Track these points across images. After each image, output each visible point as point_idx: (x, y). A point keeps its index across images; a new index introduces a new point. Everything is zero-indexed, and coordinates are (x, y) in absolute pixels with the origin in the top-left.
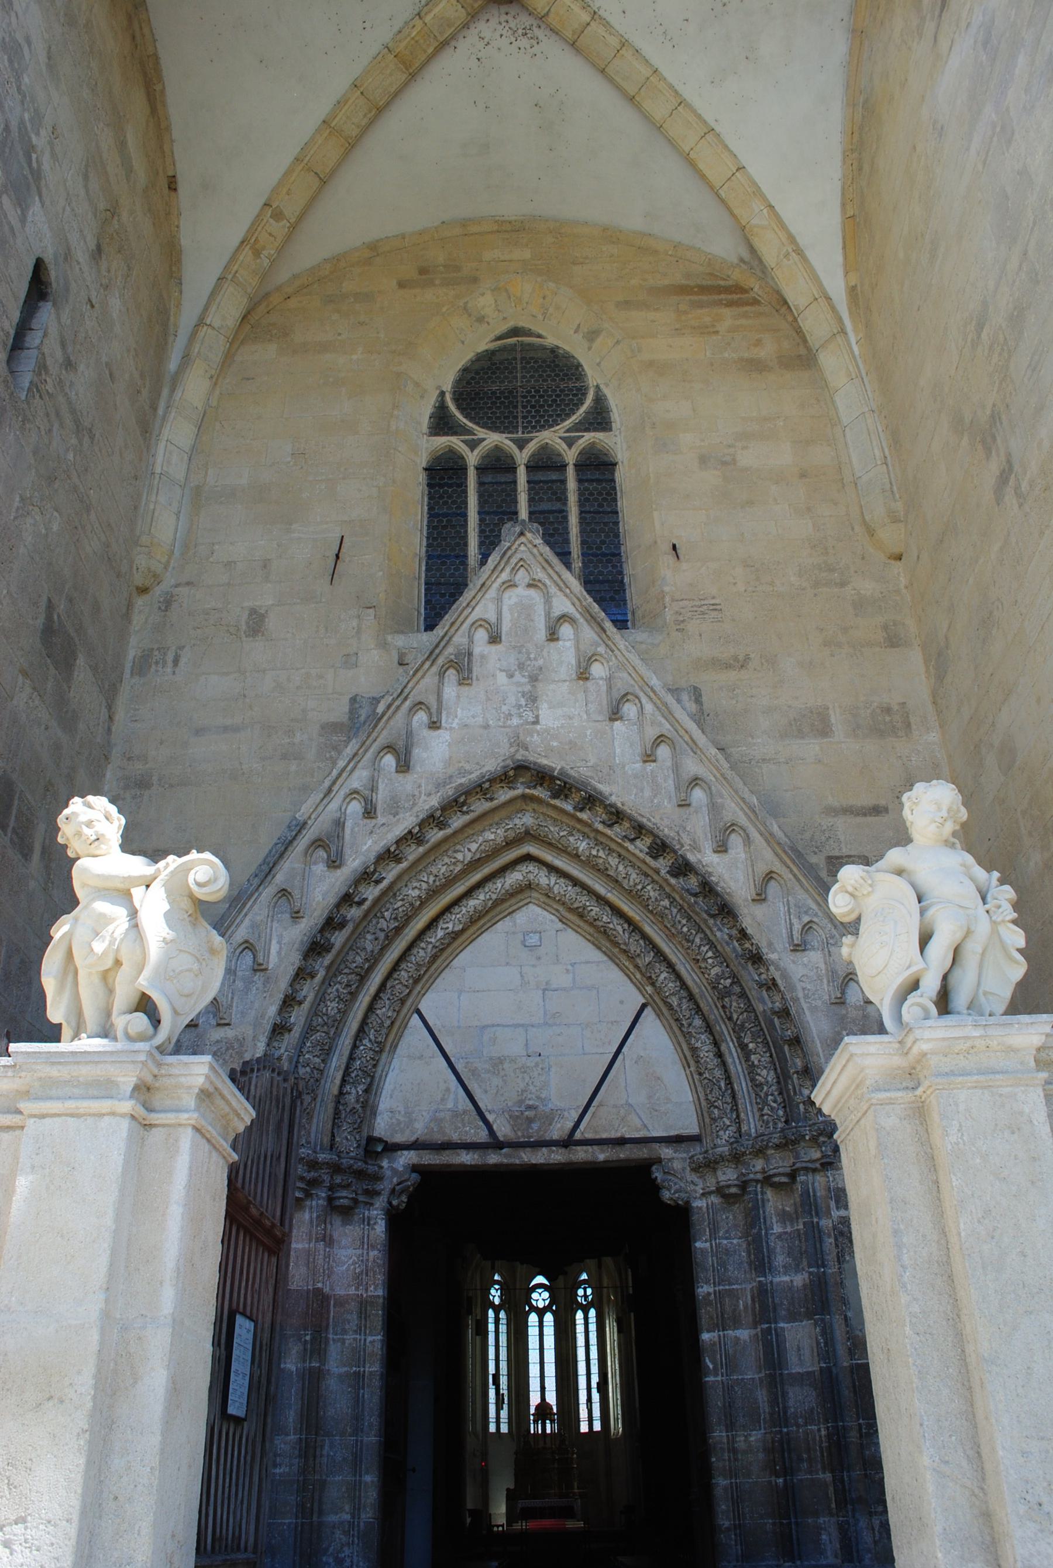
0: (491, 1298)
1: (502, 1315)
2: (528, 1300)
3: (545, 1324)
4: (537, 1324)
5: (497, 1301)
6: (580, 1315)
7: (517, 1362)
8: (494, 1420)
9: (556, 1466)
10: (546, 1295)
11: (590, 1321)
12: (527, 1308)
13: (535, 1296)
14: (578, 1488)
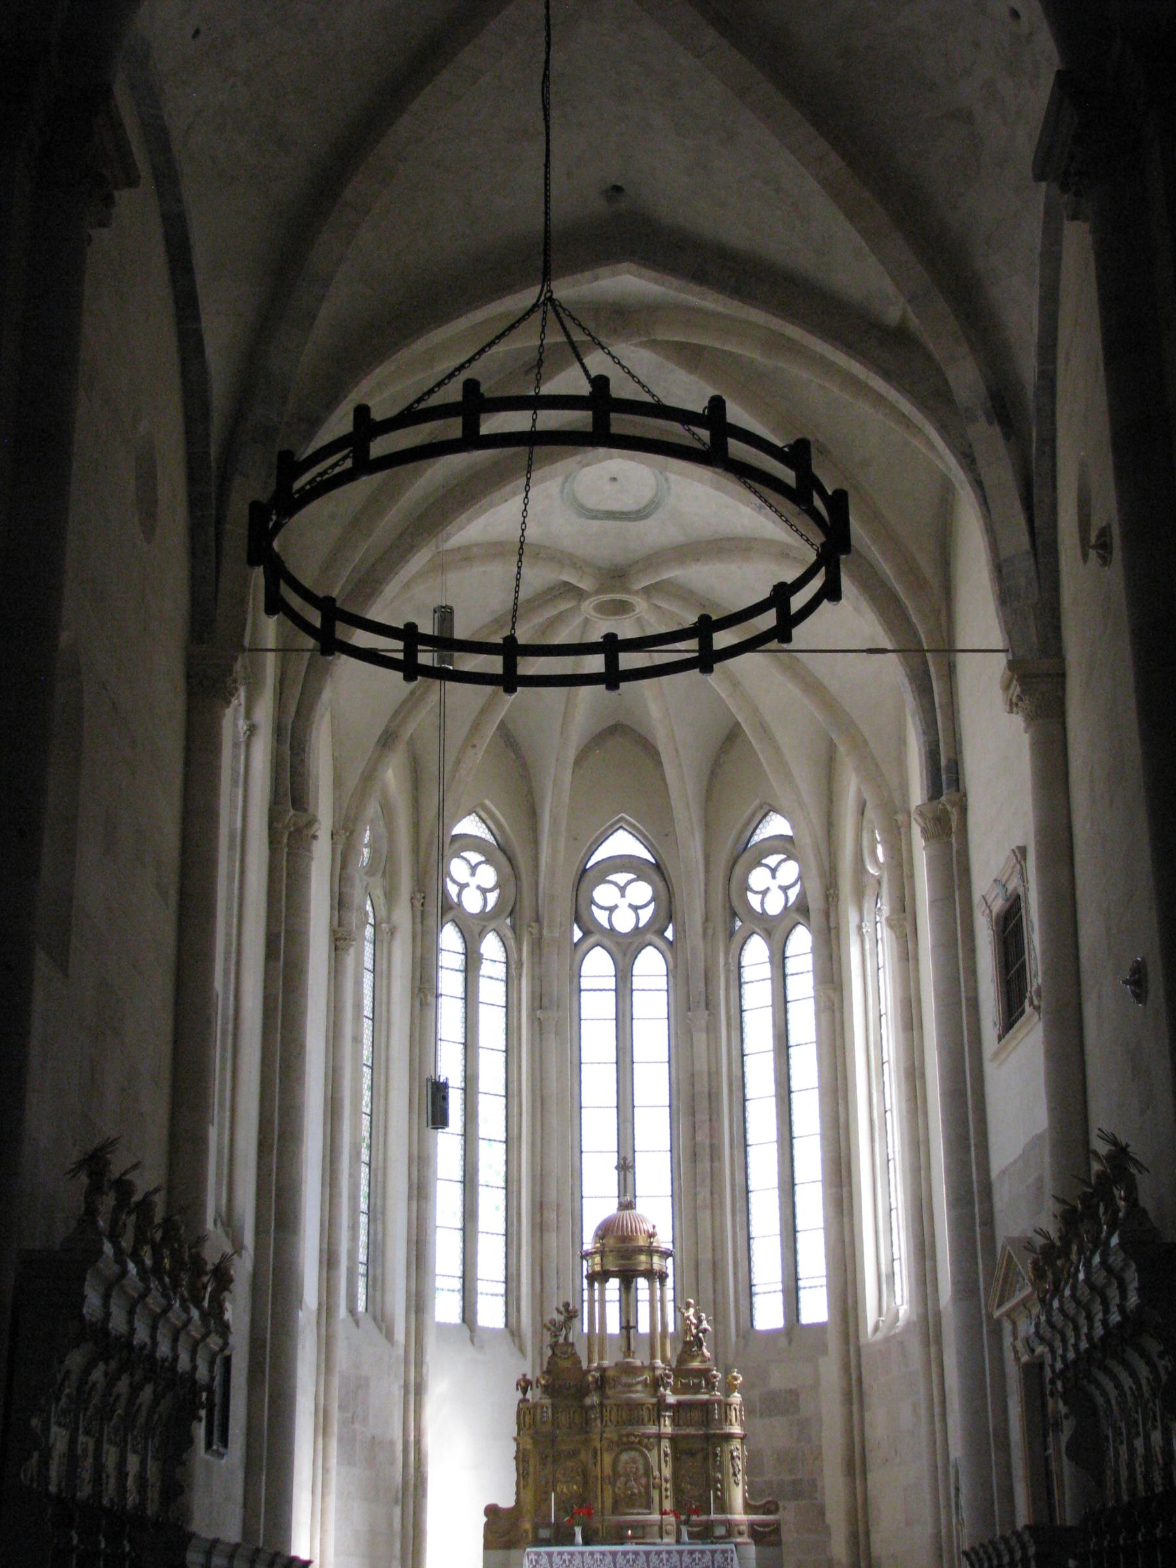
0: (453, 890)
1: (491, 947)
2: (580, 914)
3: (637, 983)
4: (611, 983)
5: (472, 903)
6: (756, 951)
7: (540, 1101)
8: (457, 1284)
9: (667, 1428)
10: (642, 892)
11: (791, 966)
12: (577, 934)
13: (604, 894)
14: (749, 1508)
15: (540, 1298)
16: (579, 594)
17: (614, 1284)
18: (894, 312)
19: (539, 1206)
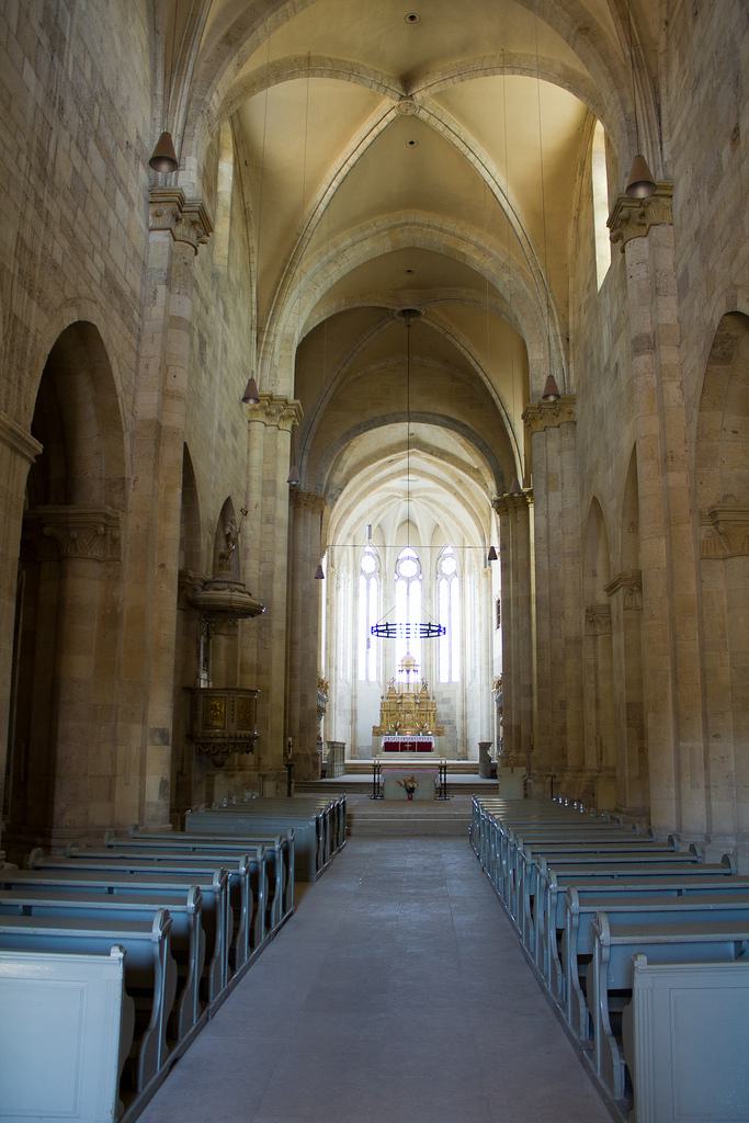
1: (373, 581)
6: (444, 583)
15: (385, 676)
16: (399, 498)
17: (405, 672)
18: (476, 467)
19: (385, 650)
